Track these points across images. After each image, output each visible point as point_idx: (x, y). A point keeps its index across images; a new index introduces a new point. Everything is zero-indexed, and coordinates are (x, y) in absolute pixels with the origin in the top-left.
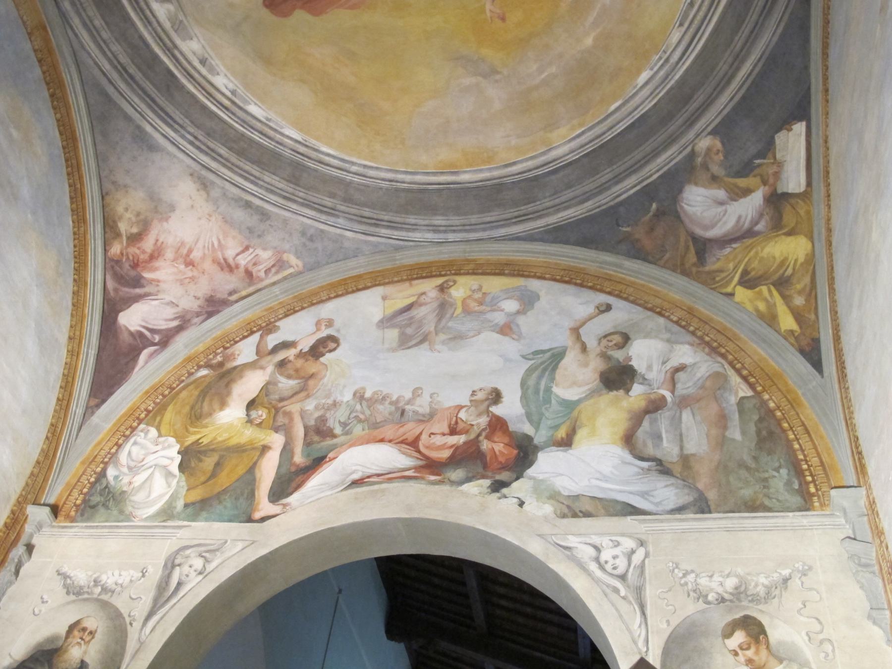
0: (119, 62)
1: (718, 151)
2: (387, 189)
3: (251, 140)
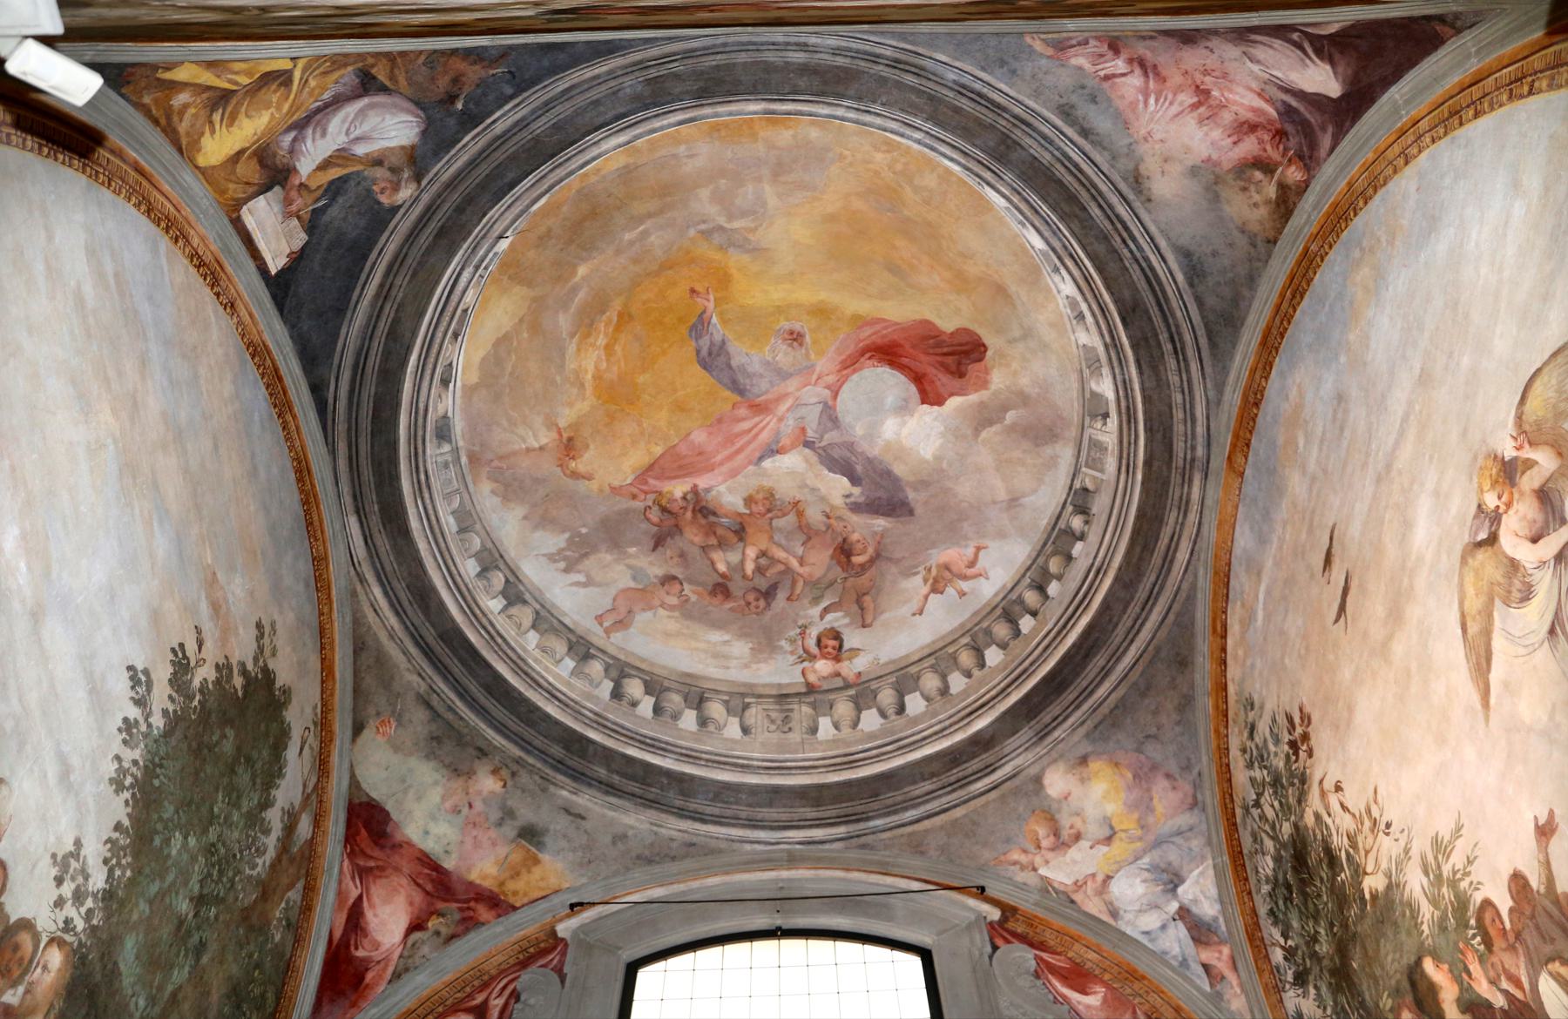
0: (1178, 362)
1: (382, 193)
2: (874, 102)
3: (1054, 210)
